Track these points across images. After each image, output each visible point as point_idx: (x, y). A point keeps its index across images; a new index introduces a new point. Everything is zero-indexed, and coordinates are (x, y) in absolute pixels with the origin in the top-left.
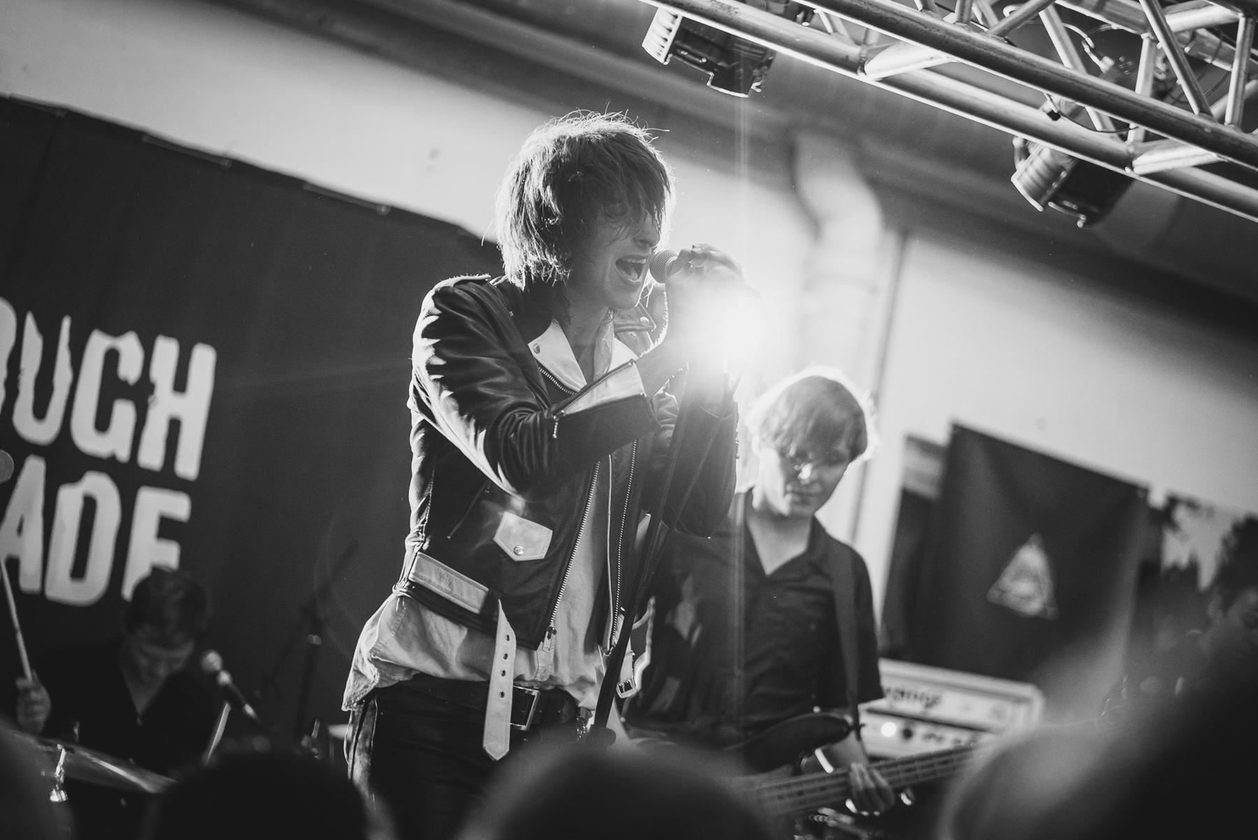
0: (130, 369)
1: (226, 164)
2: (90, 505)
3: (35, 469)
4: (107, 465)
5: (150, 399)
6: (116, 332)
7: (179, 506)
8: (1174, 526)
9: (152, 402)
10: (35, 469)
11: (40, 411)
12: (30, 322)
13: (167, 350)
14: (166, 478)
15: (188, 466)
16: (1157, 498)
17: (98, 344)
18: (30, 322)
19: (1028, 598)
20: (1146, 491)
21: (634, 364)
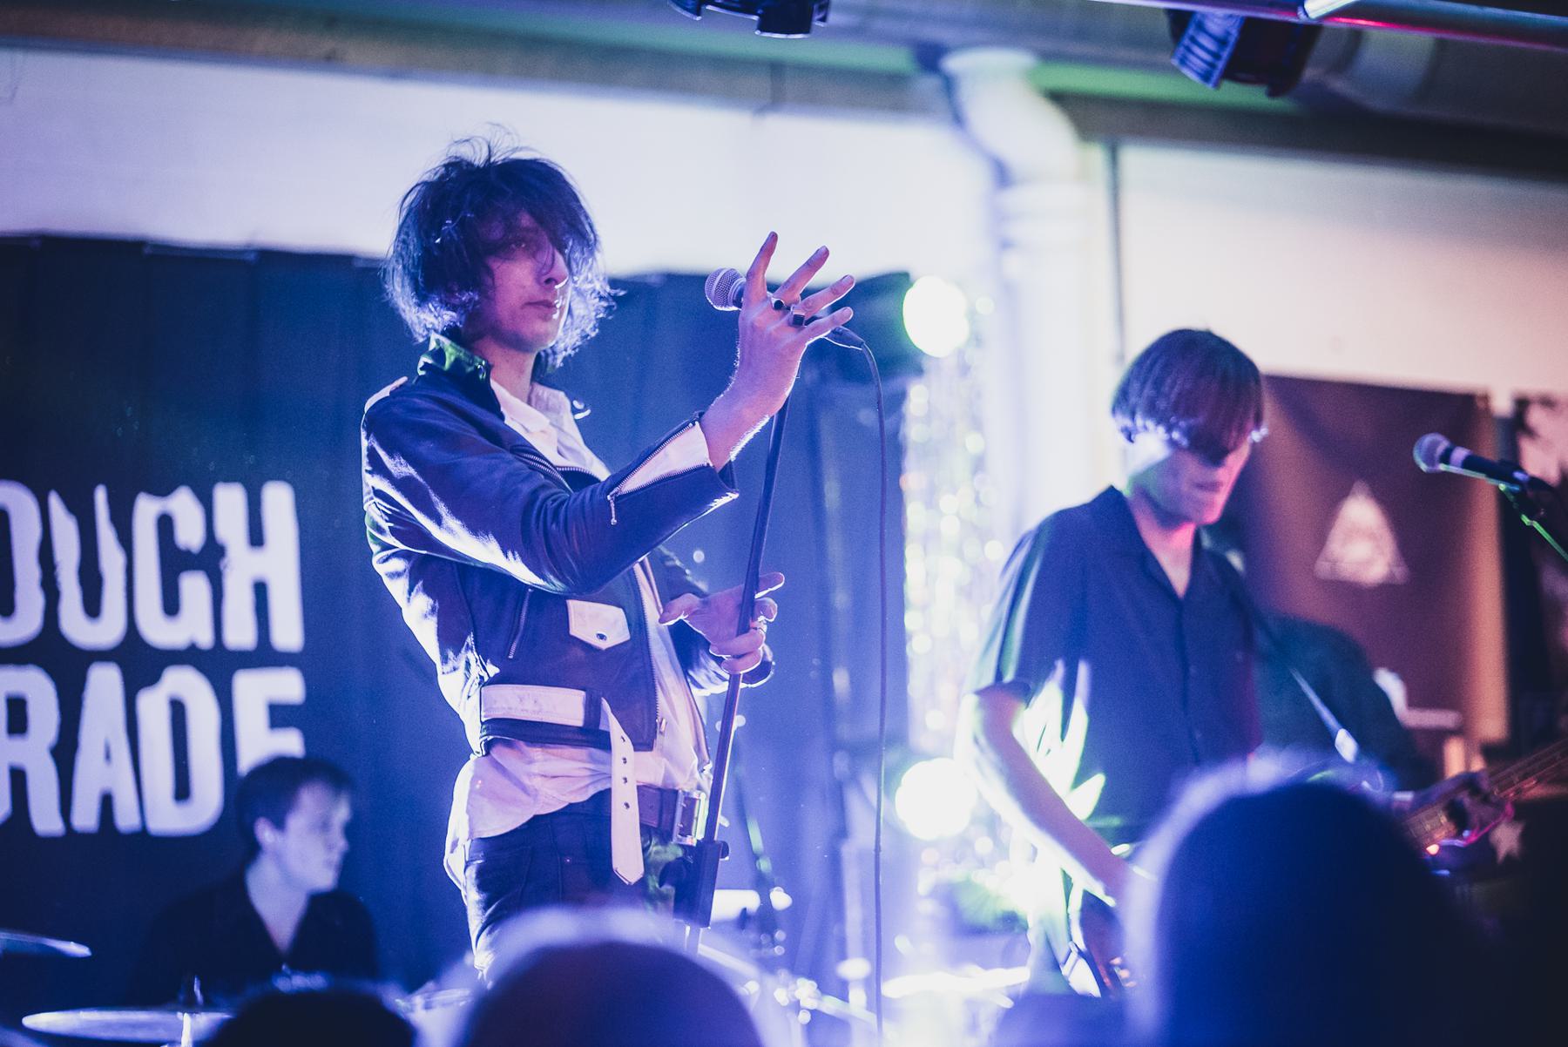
0: (190, 535)
2: (178, 711)
3: (104, 683)
4: (189, 656)
5: (225, 561)
7: (289, 686)
8: (1531, 433)
9: (225, 567)
10: (104, 683)
11: (92, 606)
12: (55, 502)
13: (230, 499)
14: (264, 656)
15: (288, 633)
16: (1502, 405)
17: (146, 510)
18: (55, 502)
19: (1368, 563)
20: (1486, 398)
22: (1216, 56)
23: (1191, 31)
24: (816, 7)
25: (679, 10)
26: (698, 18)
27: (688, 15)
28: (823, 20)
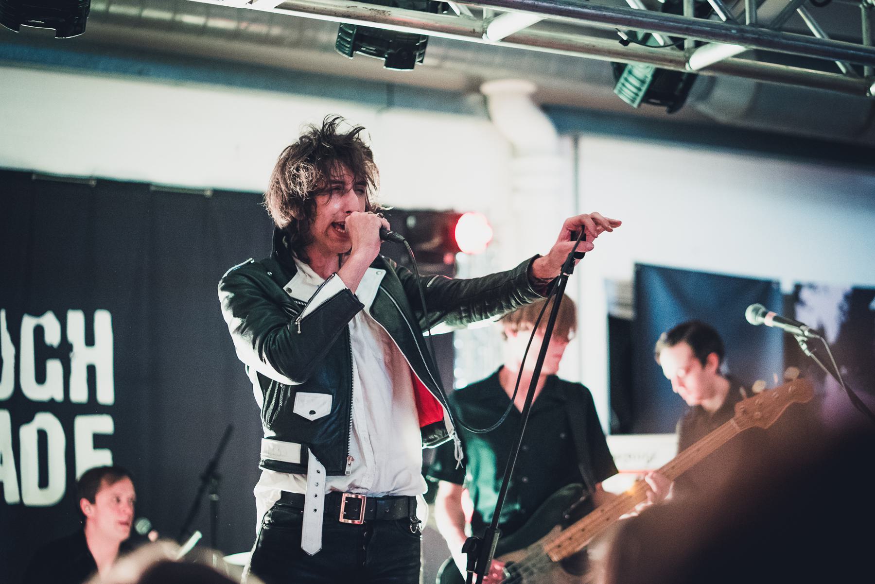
0: (53, 338)
1: (93, 183)
2: (42, 436)
4: (50, 406)
5: (71, 355)
6: (38, 314)
7: (105, 424)
8: (802, 303)
13: (76, 319)
14: (92, 407)
15: (106, 394)
16: (787, 287)
17: (28, 324)
20: (778, 284)
21: (336, 274)
22: (639, 89)
23: (625, 74)
24: (417, 54)
25: (340, 53)
26: (352, 58)
27: (346, 56)
28: (421, 61)
